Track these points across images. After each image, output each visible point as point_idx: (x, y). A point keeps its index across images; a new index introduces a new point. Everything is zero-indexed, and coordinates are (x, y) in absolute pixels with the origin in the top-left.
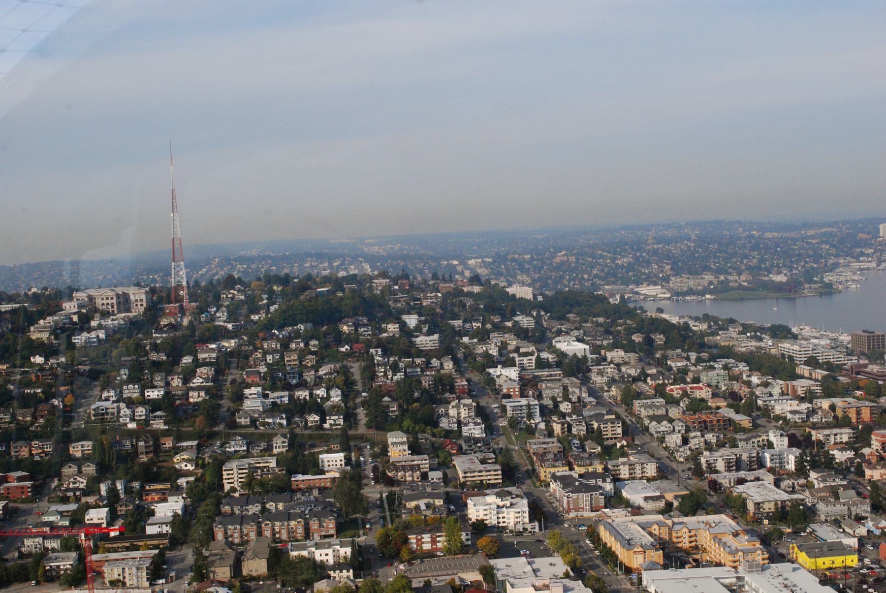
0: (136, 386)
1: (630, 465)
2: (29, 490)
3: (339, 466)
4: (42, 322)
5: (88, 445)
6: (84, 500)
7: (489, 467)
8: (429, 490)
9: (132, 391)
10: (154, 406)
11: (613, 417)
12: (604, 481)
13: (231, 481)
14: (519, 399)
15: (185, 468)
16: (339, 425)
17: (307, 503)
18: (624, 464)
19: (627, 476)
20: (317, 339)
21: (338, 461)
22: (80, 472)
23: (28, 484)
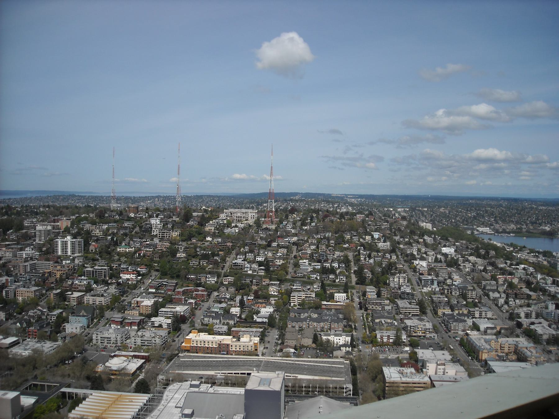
0: (252, 255)
1: (480, 312)
2: (206, 296)
3: (343, 299)
4: (211, 222)
5: (231, 279)
6: (229, 303)
7: (413, 306)
8: (386, 314)
9: (250, 256)
10: (260, 264)
11: (472, 288)
12: (468, 318)
13: (294, 301)
14: (428, 276)
15: (274, 294)
16: (344, 281)
17: (330, 315)
18: (477, 311)
19: (478, 316)
20: (334, 240)
21: (343, 297)
22: (227, 289)
23: (206, 293)
